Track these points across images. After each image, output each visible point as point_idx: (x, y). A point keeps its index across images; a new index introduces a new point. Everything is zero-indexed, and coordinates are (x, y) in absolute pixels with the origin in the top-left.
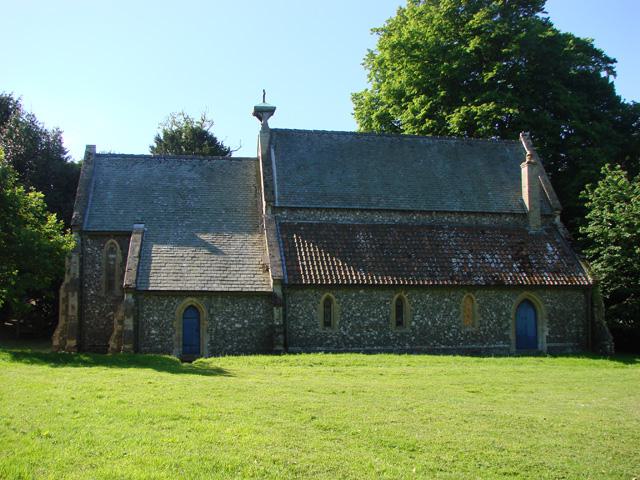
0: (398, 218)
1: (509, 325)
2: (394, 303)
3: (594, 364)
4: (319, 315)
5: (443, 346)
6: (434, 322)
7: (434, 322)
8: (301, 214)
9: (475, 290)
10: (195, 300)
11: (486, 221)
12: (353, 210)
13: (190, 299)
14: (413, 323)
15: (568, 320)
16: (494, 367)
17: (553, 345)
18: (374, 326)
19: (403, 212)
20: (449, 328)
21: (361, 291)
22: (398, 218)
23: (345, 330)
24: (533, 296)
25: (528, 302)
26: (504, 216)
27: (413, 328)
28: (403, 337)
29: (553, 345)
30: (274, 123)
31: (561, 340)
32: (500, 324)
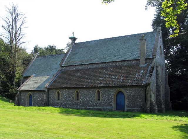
0: (95, 66)
1: (112, 101)
2: (75, 93)
3: (40, 109)
4: (56, 97)
5: (89, 107)
6: (87, 99)
7: (87, 99)
8: (69, 68)
9: (100, 88)
10: (30, 93)
11: (89, 67)
12: (83, 65)
13: (29, 93)
14: (81, 99)
15: (136, 99)
16: (156, 118)
17: (129, 108)
18: (69, 100)
19: (97, 64)
20: (91, 101)
21: (67, 90)
22: (95, 66)
23: (62, 101)
24: (122, 90)
25: (120, 92)
26: (132, 61)
27: (81, 101)
28: (77, 104)
29: (129, 108)
30: (77, 41)
31: (132, 107)
32: (109, 101)
